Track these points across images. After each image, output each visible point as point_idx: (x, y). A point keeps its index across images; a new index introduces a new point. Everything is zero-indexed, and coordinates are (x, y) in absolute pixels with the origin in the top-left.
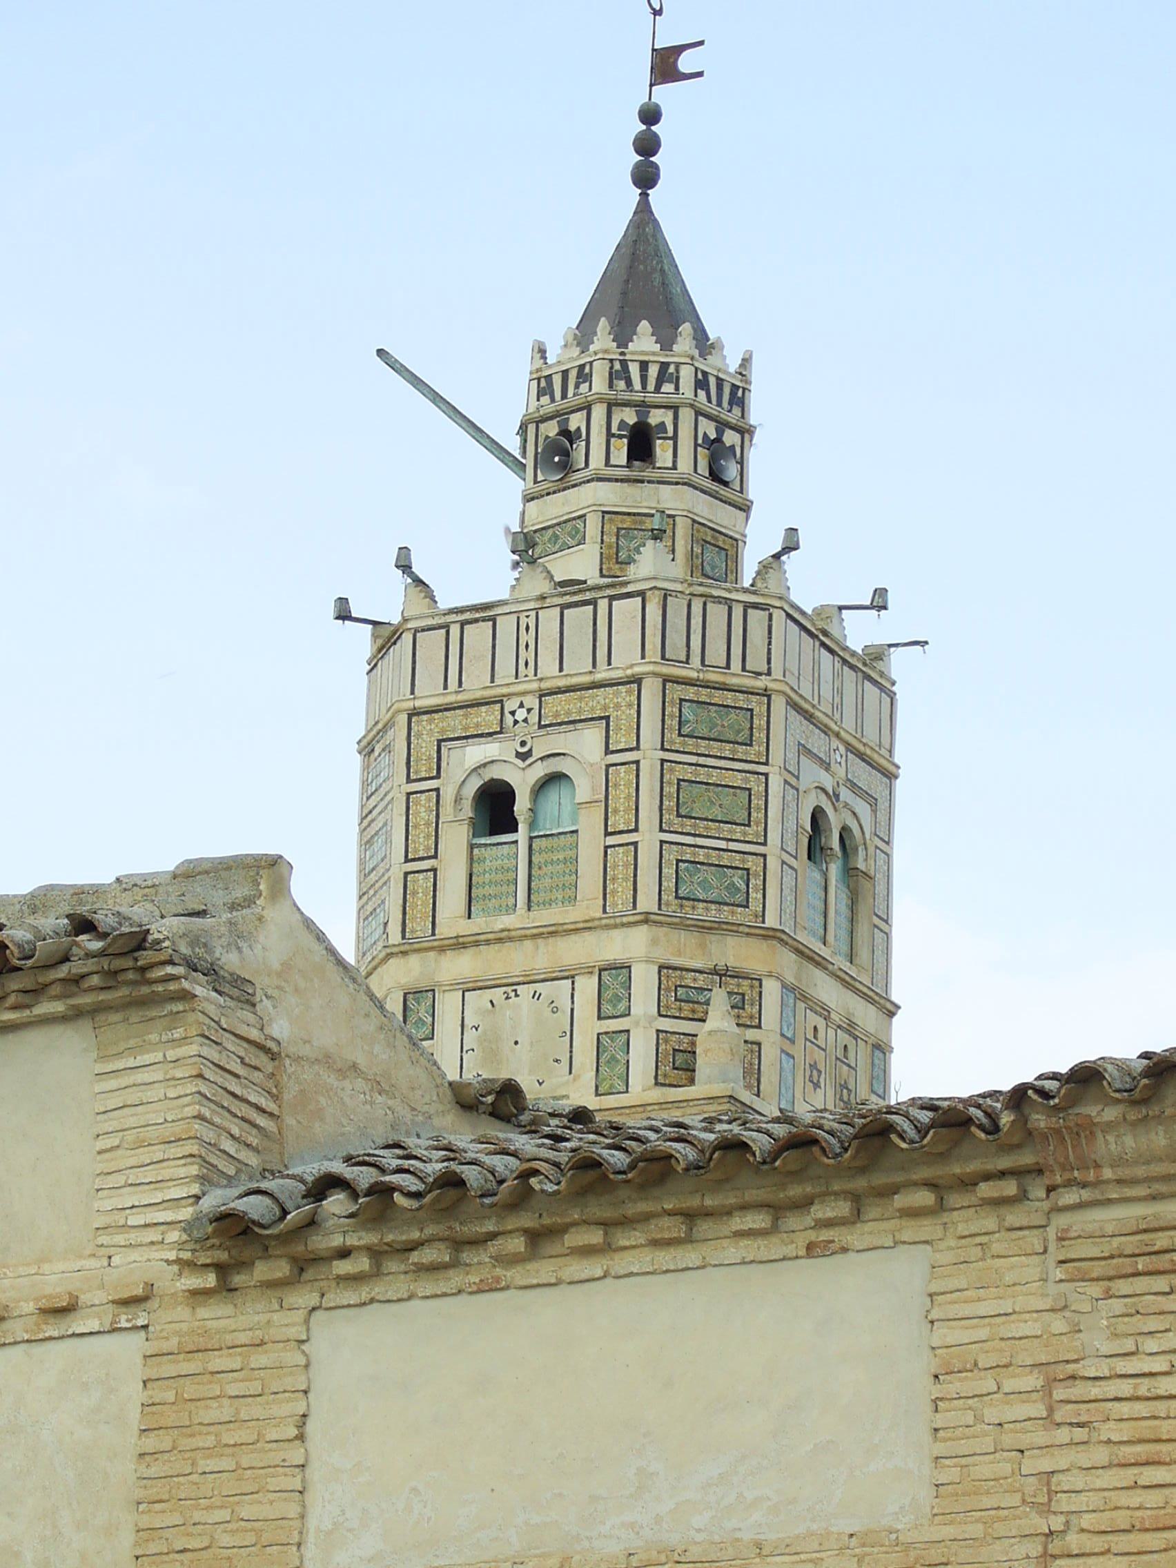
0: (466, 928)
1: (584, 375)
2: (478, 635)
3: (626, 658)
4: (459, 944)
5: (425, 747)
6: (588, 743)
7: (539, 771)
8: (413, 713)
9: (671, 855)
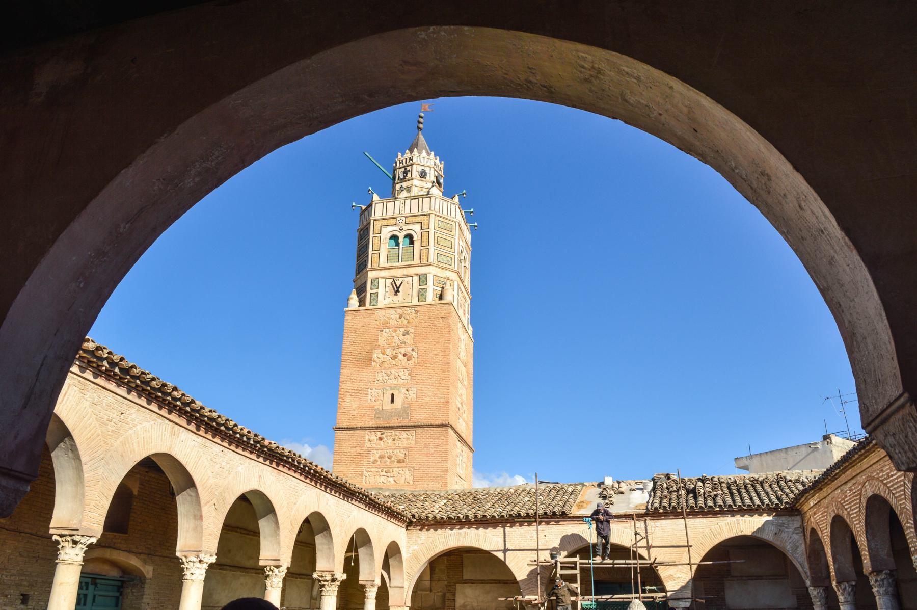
0: (386, 265)
1: (410, 159)
2: (390, 205)
3: (426, 210)
4: (385, 269)
5: (377, 227)
6: (417, 227)
7: (405, 233)
8: (375, 220)
9: (436, 252)
